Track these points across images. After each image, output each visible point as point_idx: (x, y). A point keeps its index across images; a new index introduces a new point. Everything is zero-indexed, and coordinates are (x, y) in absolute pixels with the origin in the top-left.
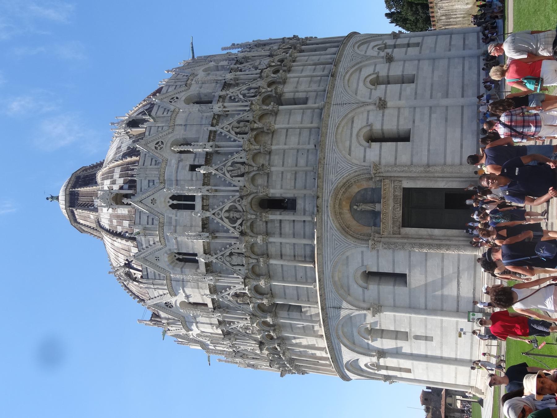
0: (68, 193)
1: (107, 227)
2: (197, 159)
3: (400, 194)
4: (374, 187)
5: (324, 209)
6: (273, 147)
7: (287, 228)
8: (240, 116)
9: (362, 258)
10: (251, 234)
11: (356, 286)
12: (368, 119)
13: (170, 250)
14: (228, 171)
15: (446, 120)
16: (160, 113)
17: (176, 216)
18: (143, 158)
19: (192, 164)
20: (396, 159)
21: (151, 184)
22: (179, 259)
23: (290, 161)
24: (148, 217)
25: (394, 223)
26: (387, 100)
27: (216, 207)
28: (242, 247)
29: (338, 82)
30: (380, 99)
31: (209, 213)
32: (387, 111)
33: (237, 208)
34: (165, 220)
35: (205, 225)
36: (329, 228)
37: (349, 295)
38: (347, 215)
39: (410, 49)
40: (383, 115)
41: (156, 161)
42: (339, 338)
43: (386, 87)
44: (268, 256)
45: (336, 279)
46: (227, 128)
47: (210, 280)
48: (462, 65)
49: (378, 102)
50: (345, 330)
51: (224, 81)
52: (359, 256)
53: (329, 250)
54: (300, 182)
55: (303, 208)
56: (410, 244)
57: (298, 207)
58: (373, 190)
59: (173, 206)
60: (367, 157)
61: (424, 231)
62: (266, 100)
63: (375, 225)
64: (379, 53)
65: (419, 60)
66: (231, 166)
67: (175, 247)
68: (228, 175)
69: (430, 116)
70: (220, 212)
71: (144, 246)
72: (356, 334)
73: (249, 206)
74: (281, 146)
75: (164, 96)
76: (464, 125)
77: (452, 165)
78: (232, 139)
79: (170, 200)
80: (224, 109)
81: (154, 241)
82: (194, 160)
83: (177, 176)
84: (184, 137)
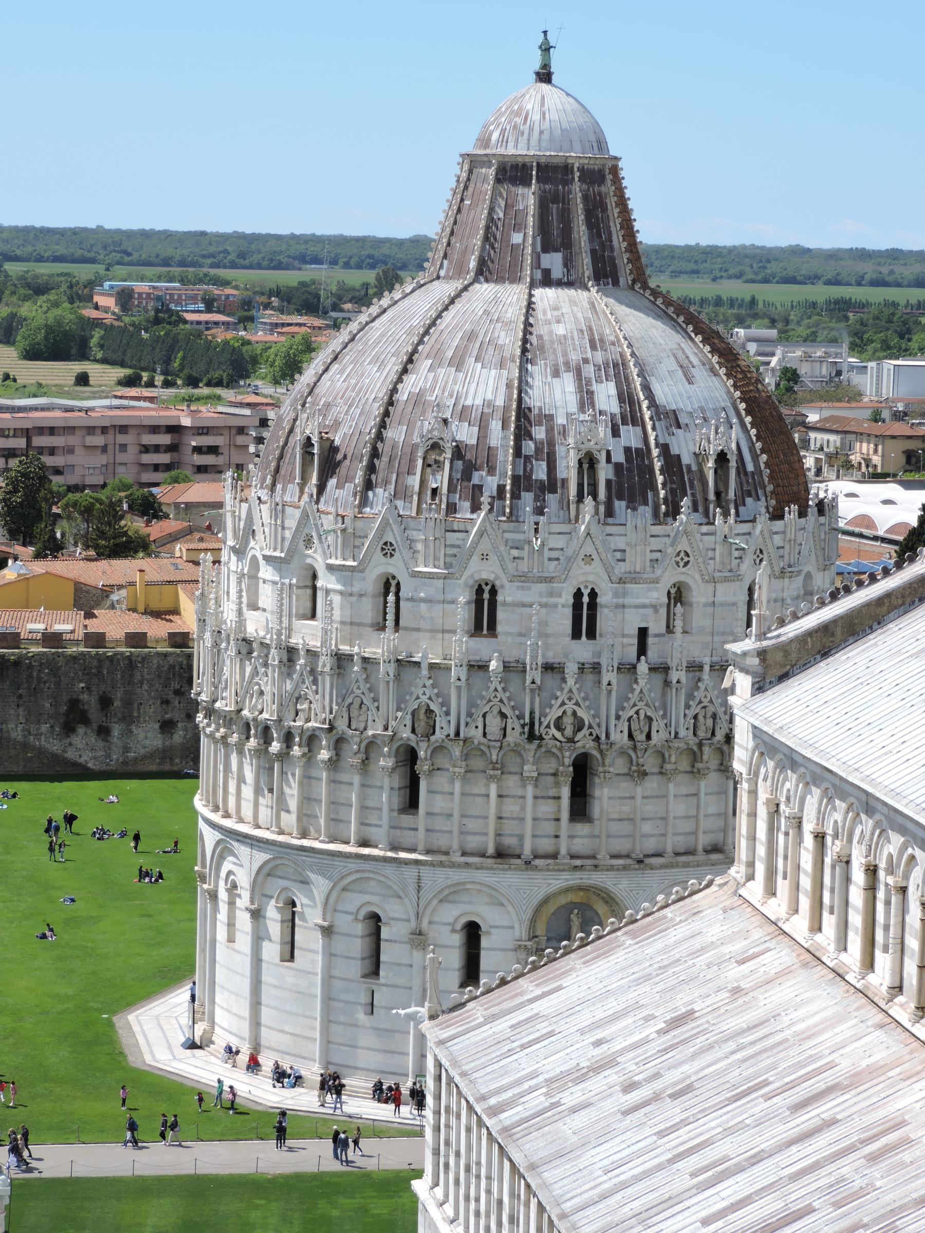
0: (570, 161)
2: (656, 640)
5: (578, 874)
8: (722, 716)
9: (503, 927)
11: (456, 913)
13: (502, 587)
14: (637, 713)
17: (563, 606)
19: (651, 632)
21: (619, 555)
23: (649, 808)
34: (555, 585)
37: (441, 901)
38: (563, 900)
42: (357, 871)
45: (468, 886)
50: (373, 883)
52: (505, 923)
54: (615, 827)
59: (578, 594)
63: (548, 940)
66: (646, 716)
67: (509, 599)
68: (632, 712)
70: (573, 701)
71: (508, 536)
72: (367, 898)
73: (583, 751)
78: (687, 712)
79: (589, 591)
82: (656, 636)
83: (630, 607)
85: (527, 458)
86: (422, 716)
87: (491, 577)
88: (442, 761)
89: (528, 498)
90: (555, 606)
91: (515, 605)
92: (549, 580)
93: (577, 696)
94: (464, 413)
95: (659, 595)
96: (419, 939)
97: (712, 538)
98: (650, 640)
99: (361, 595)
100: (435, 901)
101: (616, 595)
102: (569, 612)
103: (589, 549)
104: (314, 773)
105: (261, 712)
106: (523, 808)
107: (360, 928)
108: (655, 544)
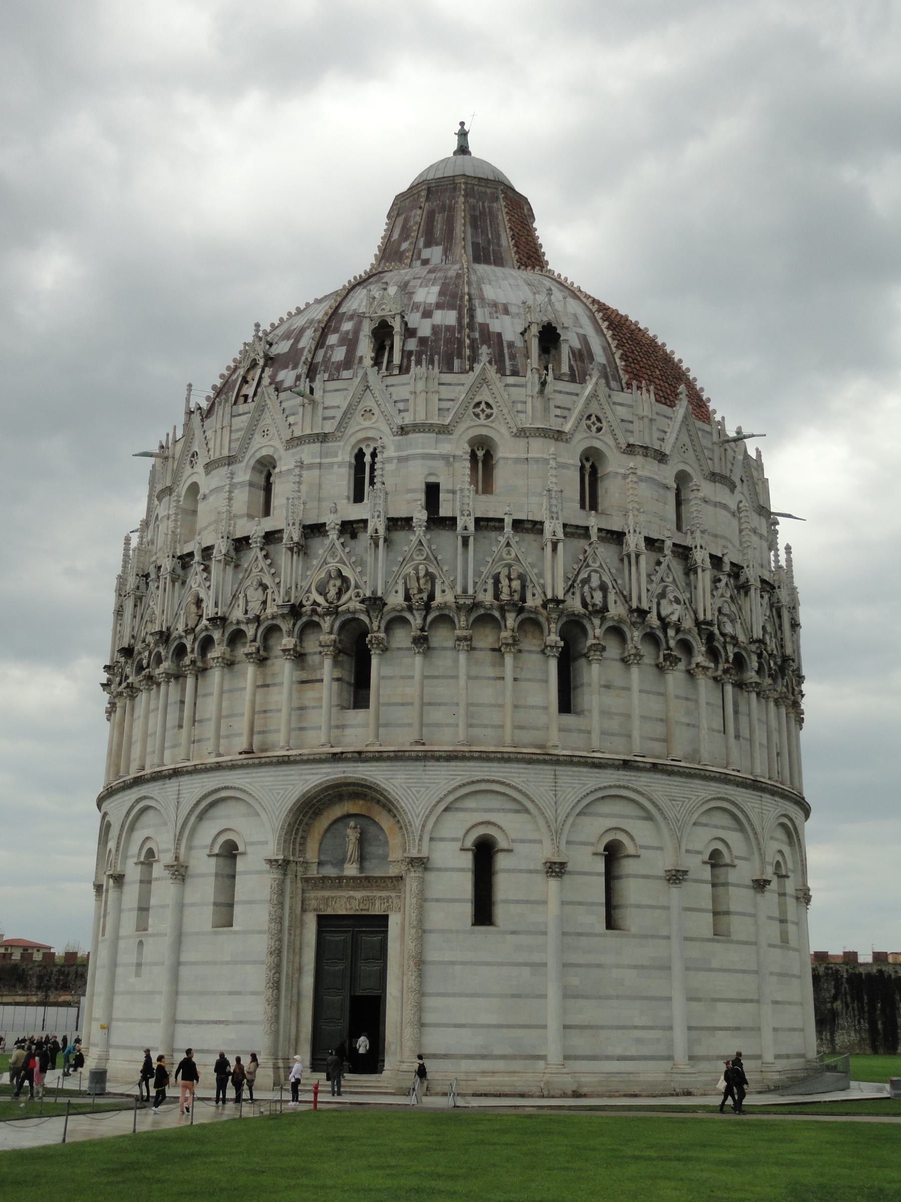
1: (342, 310)
3: (377, 910)
4: (389, 859)
7: (310, 694)
8: (534, 579)
10: (299, 623)
11: (215, 832)
12: (523, 841)
13: (280, 458)
14: (416, 569)
15: (513, 996)
16: (560, 400)
18: (455, 381)
20: (437, 900)
21: (401, 406)
22: (269, 475)
24: (338, 407)
25: (326, 900)
26: (566, 877)
27: (347, 550)
30: (562, 865)
31: (335, 537)
32: (540, 878)
33: (348, 589)
34: (330, 444)
35: (315, 530)
36: (307, 777)
39: (710, 916)
40: (530, 872)
41: (448, 409)
43: (598, 874)
44: (262, 660)
45: (223, 794)
46: (509, 553)
47: (222, 547)
48: (648, 1024)
49: (557, 860)
51: (627, 531)
53: (268, 779)
55: (346, 723)
56: (281, 931)
57: (352, 713)
58: (385, 857)
59: (360, 455)
60: (441, 845)
62: (573, 629)
63: (320, 864)
64: (699, 852)
66: (427, 573)
67: (284, 468)
68: (409, 569)
69: (526, 964)
73: (350, 616)
74: (462, 671)
75: (603, 401)
76: (504, 1030)
77: (420, 1009)
78: (482, 569)
80: (549, 545)
81: (294, 424)
82: (448, 491)
84: (501, 462)
85: (331, 347)
86: (193, 608)
90: (331, 465)
92: (323, 438)
97: (522, 390)
100: (193, 819)
101: (399, 448)
108: (445, 392)
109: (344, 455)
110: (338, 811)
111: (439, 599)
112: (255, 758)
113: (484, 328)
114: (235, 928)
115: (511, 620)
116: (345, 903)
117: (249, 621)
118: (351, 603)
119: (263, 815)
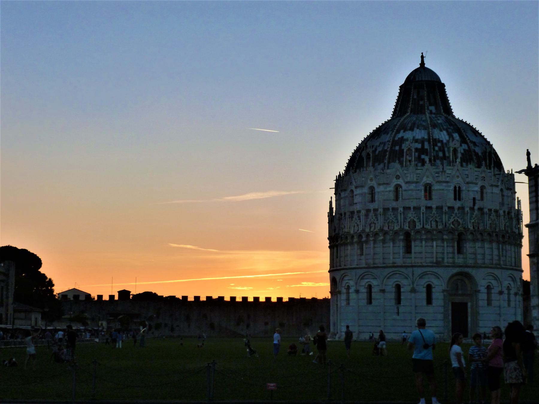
5: (461, 268)
6: (486, 243)
11: (424, 282)
19: (477, 199)
28: (440, 227)
29: (510, 272)
35: (451, 208)
37: (420, 278)
47: (423, 209)
50: (398, 275)
59: (455, 187)
61: (450, 312)
62: (503, 236)
65: (515, 307)
68: (473, 221)
71: (434, 170)
85: (437, 151)
87: (430, 182)
88: (418, 237)
89: (438, 162)
90: (449, 190)
91: (437, 190)
93: (458, 215)
94: (416, 141)
95: (477, 188)
96: (413, 291)
98: (477, 201)
99: (390, 191)
102: (453, 192)
103: (458, 174)
104: (376, 246)
105: (358, 230)
106: (443, 250)
107: (394, 290)
108: (476, 173)
109: (452, 188)
110: (455, 278)
111: (480, 228)
112: (438, 264)
113: (474, 151)
114: (434, 305)
115: (494, 234)
116: (458, 299)
117: (433, 230)
118: (460, 228)
119: (441, 279)
